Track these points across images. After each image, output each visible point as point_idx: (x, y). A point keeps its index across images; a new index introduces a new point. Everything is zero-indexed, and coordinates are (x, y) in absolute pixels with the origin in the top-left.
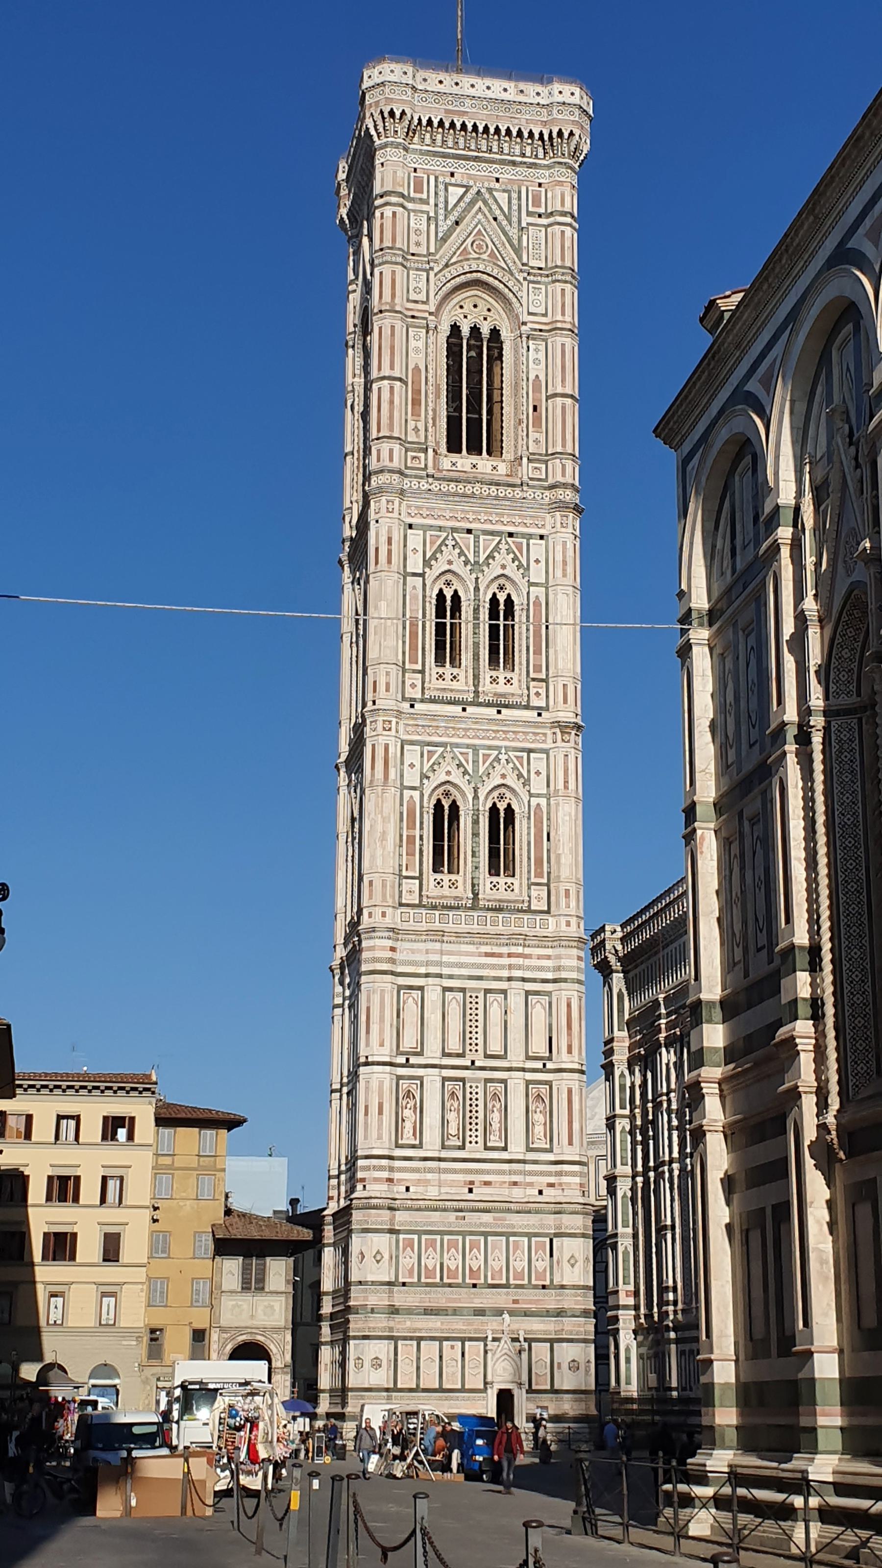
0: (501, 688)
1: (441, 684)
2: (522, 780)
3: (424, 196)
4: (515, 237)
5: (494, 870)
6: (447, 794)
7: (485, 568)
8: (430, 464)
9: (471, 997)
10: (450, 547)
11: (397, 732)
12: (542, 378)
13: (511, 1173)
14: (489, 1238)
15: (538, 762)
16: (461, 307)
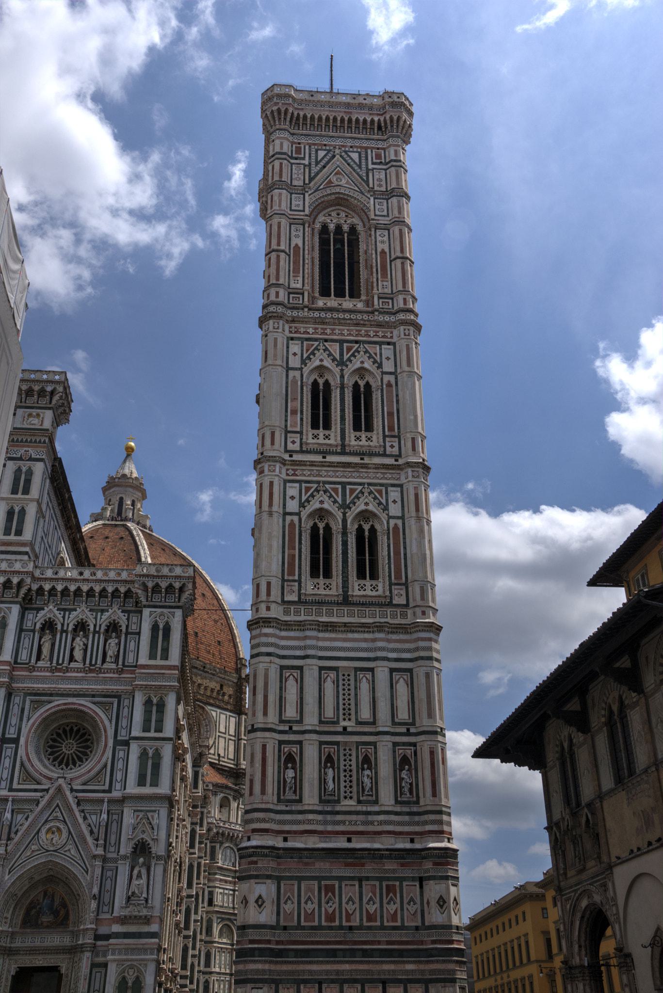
0: (363, 442)
1: (315, 441)
2: (382, 506)
3: (302, 156)
4: (364, 174)
5: (361, 575)
6: (321, 519)
7: (348, 363)
8: (306, 299)
9: (344, 675)
10: (321, 351)
11: (280, 472)
12: (387, 250)
13: (381, 823)
14: (364, 883)
15: (394, 494)
16: (330, 215)
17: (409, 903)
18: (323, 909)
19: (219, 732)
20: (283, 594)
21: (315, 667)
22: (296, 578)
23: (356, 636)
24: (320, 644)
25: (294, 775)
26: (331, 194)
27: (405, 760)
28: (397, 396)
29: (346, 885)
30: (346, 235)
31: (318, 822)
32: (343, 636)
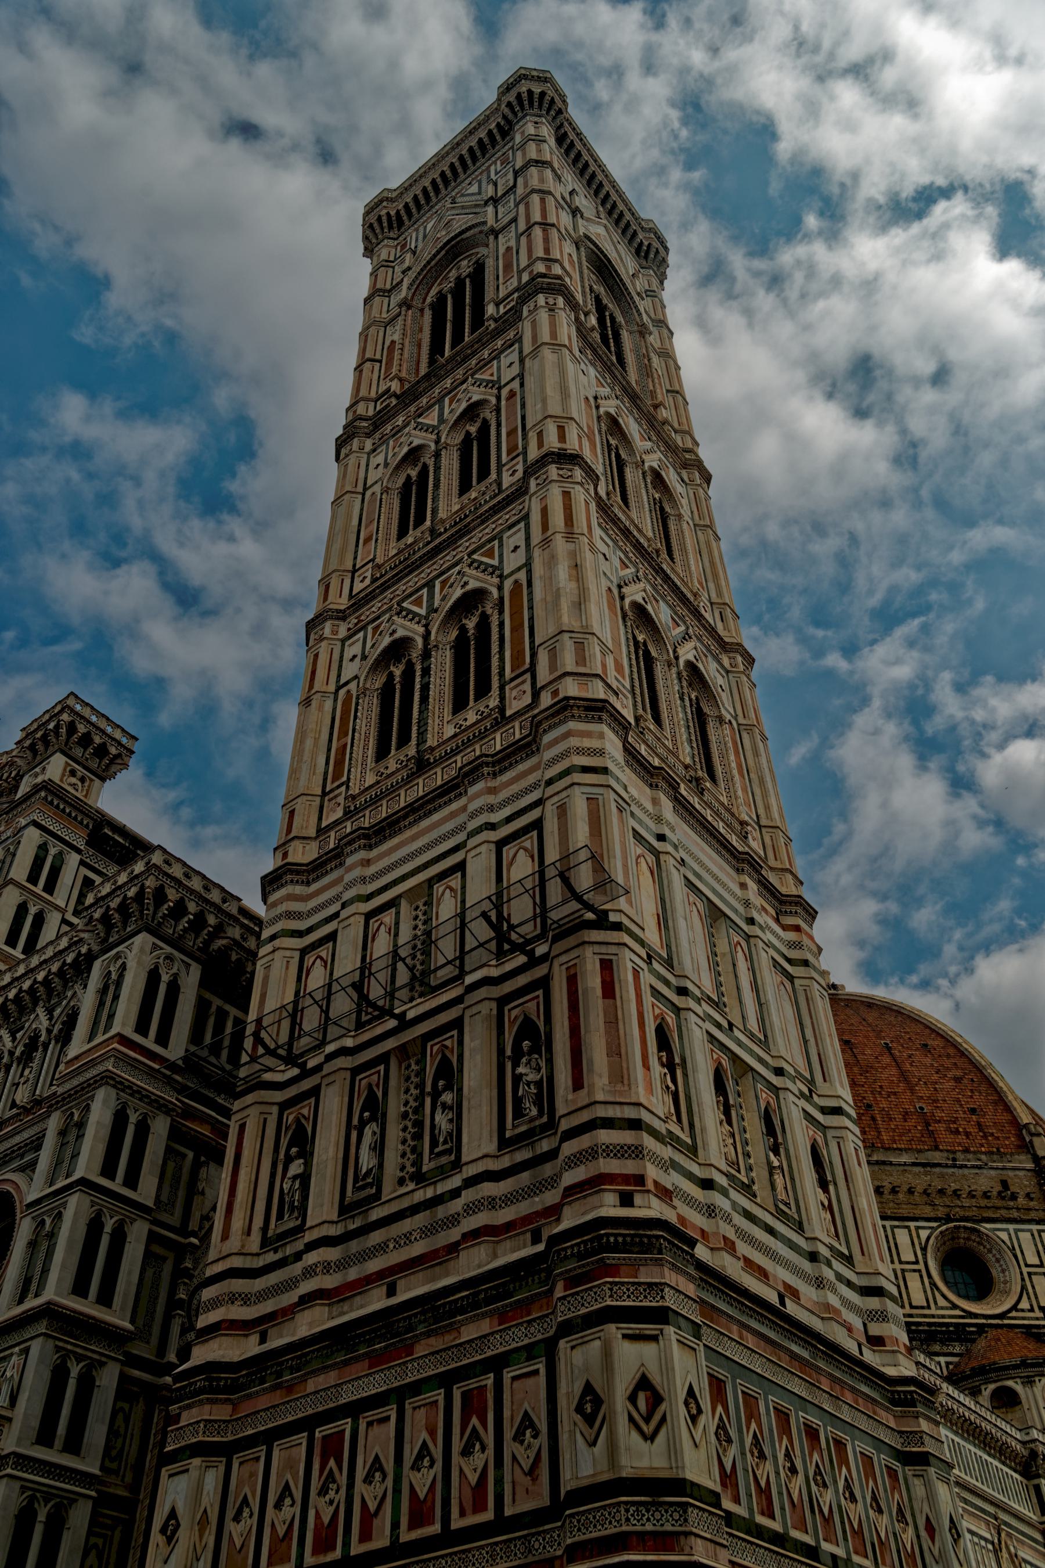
17: (519, 1437)
18: (311, 1514)
19: (1027, 1265)
20: (320, 819)
21: (352, 919)
22: (345, 779)
23: (436, 817)
24: (373, 869)
25: (300, 1170)
26: (438, 252)
27: (527, 1029)
28: (523, 398)
29: (370, 1424)
30: (468, 281)
31: (327, 1267)
32: (415, 830)
